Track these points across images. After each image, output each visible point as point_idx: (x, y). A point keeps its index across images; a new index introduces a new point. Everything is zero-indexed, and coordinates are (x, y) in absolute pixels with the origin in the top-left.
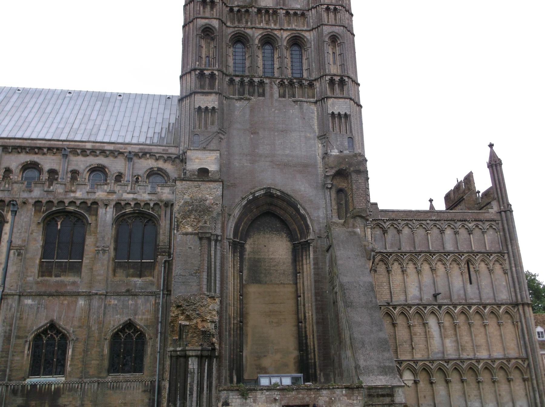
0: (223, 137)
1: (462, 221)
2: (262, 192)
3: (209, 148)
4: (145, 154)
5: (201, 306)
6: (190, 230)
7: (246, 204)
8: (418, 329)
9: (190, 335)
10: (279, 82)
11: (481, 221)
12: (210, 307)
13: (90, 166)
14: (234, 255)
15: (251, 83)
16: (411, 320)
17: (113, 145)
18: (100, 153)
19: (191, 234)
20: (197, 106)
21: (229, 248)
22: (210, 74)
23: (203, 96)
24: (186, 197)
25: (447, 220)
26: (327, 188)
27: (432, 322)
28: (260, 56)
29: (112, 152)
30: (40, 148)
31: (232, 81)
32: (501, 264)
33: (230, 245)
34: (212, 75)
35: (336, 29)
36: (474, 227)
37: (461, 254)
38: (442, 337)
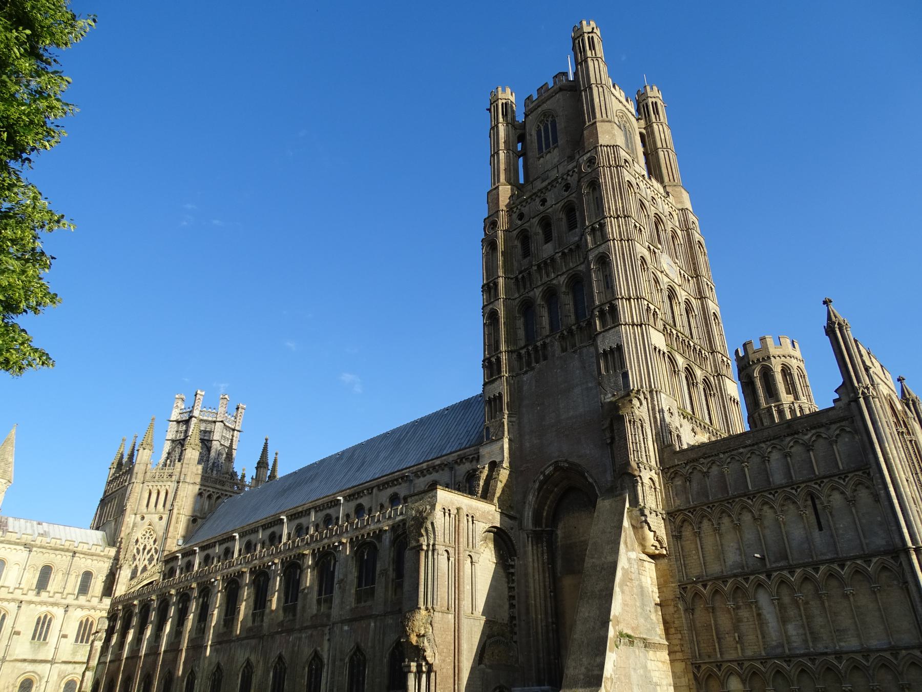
1: (792, 434)
2: (551, 468)
7: (539, 486)
10: (559, 337)
11: (822, 426)
14: (537, 547)
15: (536, 348)
16: (729, 601)
17: (440, 459)
21: (528, 541)
25: (767, 441)
26: (607, 444)
27: (763, 599)
28: (546, 314)
29: (439, 465)
30: (397, 480)
32: (867, 487)
33: (528, 537)
36: (814, 438)
38: (783, 620)
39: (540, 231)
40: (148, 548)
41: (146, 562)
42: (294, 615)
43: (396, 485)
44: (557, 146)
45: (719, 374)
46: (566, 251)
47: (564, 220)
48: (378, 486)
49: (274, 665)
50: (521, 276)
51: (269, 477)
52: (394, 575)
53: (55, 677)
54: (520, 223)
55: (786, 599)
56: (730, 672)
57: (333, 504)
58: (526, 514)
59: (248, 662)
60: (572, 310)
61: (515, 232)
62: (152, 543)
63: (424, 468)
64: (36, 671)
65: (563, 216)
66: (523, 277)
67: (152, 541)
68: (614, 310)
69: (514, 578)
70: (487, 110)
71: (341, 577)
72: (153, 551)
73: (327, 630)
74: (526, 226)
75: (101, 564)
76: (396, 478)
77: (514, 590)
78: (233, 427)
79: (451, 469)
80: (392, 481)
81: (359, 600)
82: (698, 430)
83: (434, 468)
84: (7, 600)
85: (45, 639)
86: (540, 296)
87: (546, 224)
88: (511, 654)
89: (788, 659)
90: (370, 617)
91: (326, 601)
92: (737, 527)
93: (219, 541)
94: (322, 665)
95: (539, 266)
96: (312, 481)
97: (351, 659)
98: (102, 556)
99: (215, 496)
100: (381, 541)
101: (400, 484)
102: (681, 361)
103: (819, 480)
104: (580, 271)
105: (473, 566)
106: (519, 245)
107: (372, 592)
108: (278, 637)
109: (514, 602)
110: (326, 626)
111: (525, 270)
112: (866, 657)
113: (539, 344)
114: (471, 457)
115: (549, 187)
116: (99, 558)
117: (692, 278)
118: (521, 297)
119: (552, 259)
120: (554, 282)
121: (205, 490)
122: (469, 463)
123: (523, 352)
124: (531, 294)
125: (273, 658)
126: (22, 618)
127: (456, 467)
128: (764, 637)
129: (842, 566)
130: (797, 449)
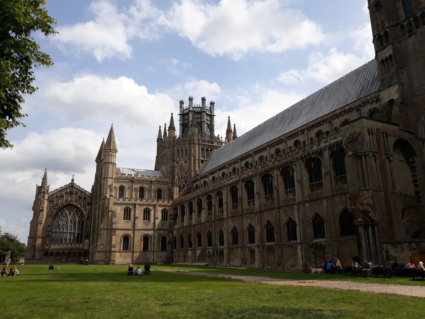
0: (402, 70)
3: (391, 85)
4: (364, 103)
5: (359, 197)
6: (351, 153)
9: (358, 214)
12: (366, 196)
13: (341, 122)
17: (348, 106)
18: (344, 113)
19: (352, 155)
20: (380, 60)
22: (384, 33)
23: (382, 51)
24: (347, 134)
29: (348, 110)
30: (320, 123)
31: (402, 27)
34: (386, 33)
40: (183, 176)
41: (184, 183)
42: (272, 200)
43: (319, 126)
48: (307, 129)
49: (265, 226)
51: (233, 137)
52: (335, 174)
53: (157, 236)
57: (280, 142)
58: (420, 129)
59: (250, 225)
62: (185, 174)
63: (338, 113)
64: (148, 233)
67: (184, 173)
69: (415, 169)
71: (299, 178)
72: (186, 178)
73: (295, 207)
75: (164, 186)
76: (319, 122)
77: (416, 176)
78: (210, 114)
79: (358, 110)
80: (317, 124)
81: (312, 189)
83: (345, 112)
84: (129, 204)
85: (149, 220)
88: (419, 213)
90: (323, 198)
91: (290, 192)
93: (218, 169)
94: (295, 225)
96: (262, 134)
97: (313, 221)
98: (164, 182)
99: (210, 149)
100: (323, 156)
101: (322, 125)
105: (391, 163)
107: (321, 185)
108: (265, 212)
109: (418, 183)
110: (294, 205)
113: (418, 15)
114: (371, 101)
116: (163, 183)
121: (204, 147)
122: (370, 105)
123: (405, 23)
125: (265, 223)
126: (137, 211)
127: (361, 109)
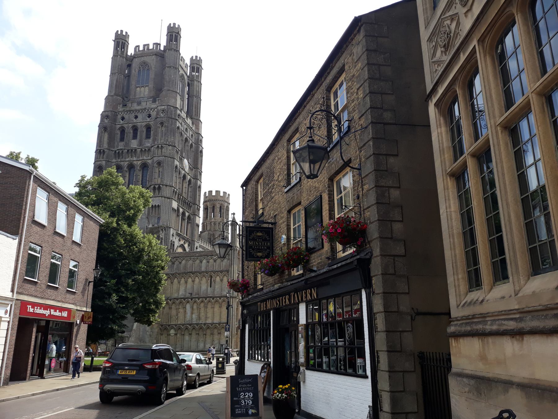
8: (181, 310)
27: (188, 306)
35: (161, 158)
37: (207, 272)
38: (192, 313)
39: (132, 132)
44: (148, 86)
45: (194, 214)
46: (143, 149)
47: (145, 132)
50: (117, 151)
54: (122, 122)
55: (195, 307)
56: (172, 328)
60: (141, 179)
61: (118, 126)
65: (145, 130)
66: (119, 152)
68: (159, 188)
70: (113, 40)
74: (125, 126)
82: (181, 239)
86: (127, 166)
87: (135, 129)
89: (190, 325)
92: (186, 282)
95: (128, 150)
102: (181, 210)
103: (214, 272)
104: (148, 163)
106: (119, 133)
111: (121, 149)
112: (212, 325)
115: (141, 111)
117: (194, 168)
118: (117, 163)
119: (136, 150)
120: (135, 162)
124: (122, 163)
128: (185, 318)
129: (213, 299)
130: (211, 261)
